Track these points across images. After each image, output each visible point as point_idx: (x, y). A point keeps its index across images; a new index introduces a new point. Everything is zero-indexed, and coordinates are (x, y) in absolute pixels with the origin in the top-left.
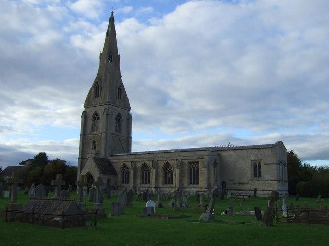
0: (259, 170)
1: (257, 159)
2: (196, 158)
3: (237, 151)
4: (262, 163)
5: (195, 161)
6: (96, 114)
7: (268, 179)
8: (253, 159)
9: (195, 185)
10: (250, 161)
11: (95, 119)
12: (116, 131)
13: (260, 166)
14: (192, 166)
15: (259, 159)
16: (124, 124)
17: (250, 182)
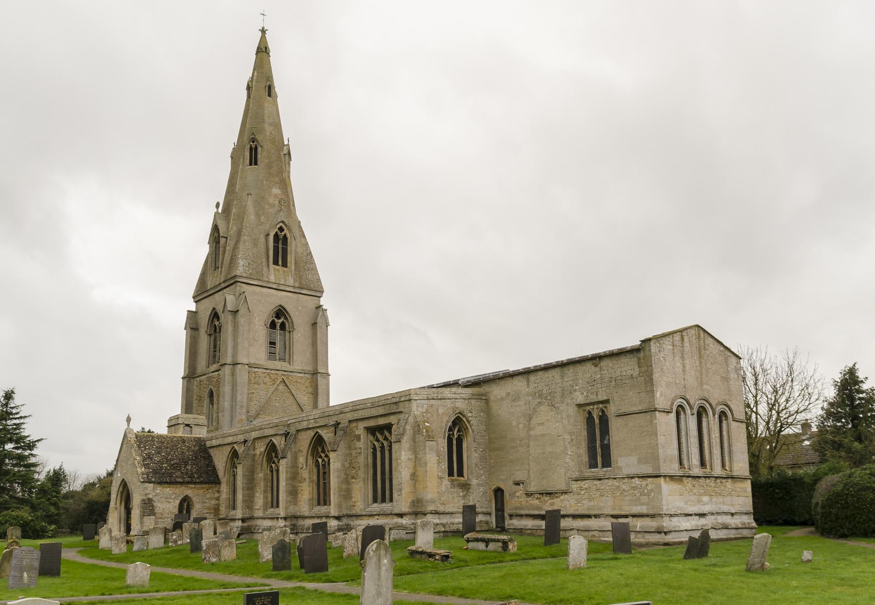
0: (602, 440)
1: (593, 398)
2: (381, 411)
3: (532, 378)
4: (612, 410)
5: (382, 421)
6: (281, 311)
7: (633, 471)
8: (581, 399)
9: (384, 505)
10: (572, 410)
11: (273, 325)
12: (272, 355)
13: (604, 421)
14: (378, 440)
15: (601, 398)
16: (300, 336)
17: (575, 486)
